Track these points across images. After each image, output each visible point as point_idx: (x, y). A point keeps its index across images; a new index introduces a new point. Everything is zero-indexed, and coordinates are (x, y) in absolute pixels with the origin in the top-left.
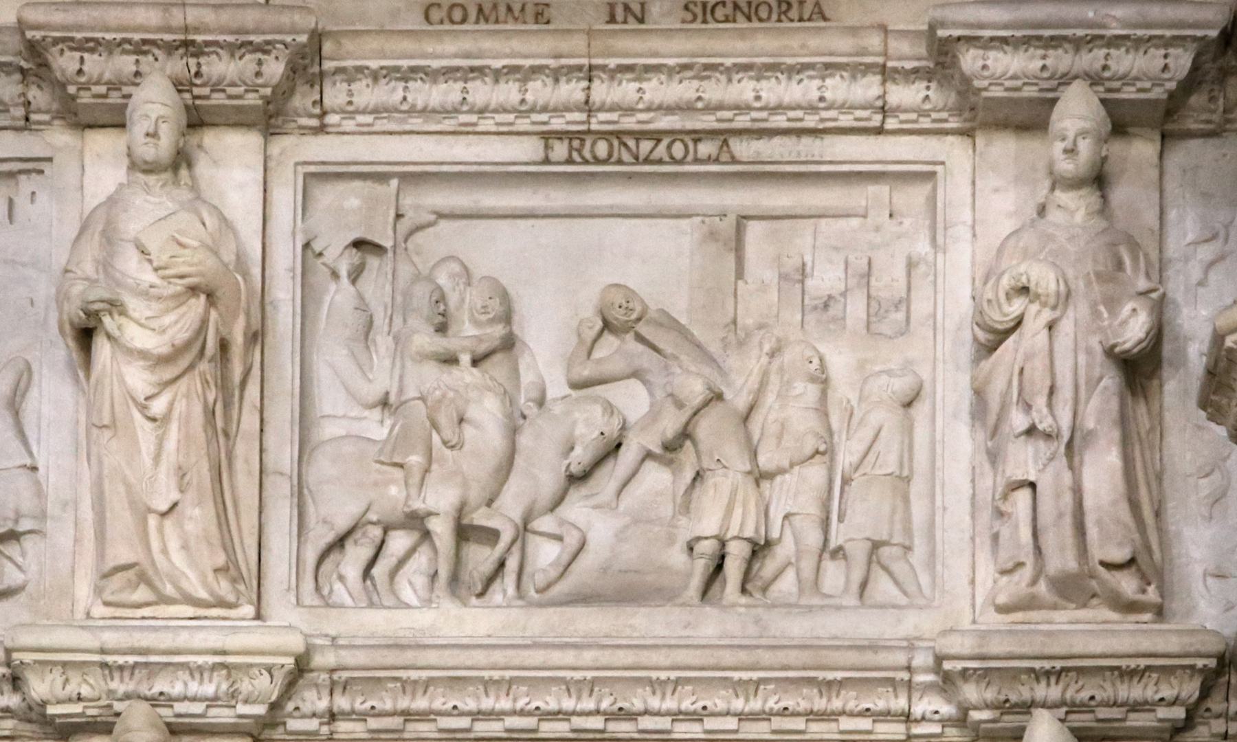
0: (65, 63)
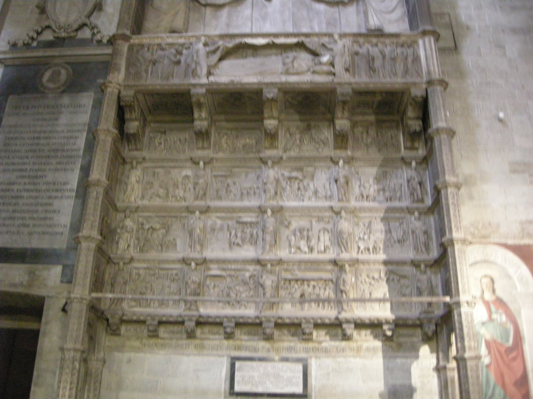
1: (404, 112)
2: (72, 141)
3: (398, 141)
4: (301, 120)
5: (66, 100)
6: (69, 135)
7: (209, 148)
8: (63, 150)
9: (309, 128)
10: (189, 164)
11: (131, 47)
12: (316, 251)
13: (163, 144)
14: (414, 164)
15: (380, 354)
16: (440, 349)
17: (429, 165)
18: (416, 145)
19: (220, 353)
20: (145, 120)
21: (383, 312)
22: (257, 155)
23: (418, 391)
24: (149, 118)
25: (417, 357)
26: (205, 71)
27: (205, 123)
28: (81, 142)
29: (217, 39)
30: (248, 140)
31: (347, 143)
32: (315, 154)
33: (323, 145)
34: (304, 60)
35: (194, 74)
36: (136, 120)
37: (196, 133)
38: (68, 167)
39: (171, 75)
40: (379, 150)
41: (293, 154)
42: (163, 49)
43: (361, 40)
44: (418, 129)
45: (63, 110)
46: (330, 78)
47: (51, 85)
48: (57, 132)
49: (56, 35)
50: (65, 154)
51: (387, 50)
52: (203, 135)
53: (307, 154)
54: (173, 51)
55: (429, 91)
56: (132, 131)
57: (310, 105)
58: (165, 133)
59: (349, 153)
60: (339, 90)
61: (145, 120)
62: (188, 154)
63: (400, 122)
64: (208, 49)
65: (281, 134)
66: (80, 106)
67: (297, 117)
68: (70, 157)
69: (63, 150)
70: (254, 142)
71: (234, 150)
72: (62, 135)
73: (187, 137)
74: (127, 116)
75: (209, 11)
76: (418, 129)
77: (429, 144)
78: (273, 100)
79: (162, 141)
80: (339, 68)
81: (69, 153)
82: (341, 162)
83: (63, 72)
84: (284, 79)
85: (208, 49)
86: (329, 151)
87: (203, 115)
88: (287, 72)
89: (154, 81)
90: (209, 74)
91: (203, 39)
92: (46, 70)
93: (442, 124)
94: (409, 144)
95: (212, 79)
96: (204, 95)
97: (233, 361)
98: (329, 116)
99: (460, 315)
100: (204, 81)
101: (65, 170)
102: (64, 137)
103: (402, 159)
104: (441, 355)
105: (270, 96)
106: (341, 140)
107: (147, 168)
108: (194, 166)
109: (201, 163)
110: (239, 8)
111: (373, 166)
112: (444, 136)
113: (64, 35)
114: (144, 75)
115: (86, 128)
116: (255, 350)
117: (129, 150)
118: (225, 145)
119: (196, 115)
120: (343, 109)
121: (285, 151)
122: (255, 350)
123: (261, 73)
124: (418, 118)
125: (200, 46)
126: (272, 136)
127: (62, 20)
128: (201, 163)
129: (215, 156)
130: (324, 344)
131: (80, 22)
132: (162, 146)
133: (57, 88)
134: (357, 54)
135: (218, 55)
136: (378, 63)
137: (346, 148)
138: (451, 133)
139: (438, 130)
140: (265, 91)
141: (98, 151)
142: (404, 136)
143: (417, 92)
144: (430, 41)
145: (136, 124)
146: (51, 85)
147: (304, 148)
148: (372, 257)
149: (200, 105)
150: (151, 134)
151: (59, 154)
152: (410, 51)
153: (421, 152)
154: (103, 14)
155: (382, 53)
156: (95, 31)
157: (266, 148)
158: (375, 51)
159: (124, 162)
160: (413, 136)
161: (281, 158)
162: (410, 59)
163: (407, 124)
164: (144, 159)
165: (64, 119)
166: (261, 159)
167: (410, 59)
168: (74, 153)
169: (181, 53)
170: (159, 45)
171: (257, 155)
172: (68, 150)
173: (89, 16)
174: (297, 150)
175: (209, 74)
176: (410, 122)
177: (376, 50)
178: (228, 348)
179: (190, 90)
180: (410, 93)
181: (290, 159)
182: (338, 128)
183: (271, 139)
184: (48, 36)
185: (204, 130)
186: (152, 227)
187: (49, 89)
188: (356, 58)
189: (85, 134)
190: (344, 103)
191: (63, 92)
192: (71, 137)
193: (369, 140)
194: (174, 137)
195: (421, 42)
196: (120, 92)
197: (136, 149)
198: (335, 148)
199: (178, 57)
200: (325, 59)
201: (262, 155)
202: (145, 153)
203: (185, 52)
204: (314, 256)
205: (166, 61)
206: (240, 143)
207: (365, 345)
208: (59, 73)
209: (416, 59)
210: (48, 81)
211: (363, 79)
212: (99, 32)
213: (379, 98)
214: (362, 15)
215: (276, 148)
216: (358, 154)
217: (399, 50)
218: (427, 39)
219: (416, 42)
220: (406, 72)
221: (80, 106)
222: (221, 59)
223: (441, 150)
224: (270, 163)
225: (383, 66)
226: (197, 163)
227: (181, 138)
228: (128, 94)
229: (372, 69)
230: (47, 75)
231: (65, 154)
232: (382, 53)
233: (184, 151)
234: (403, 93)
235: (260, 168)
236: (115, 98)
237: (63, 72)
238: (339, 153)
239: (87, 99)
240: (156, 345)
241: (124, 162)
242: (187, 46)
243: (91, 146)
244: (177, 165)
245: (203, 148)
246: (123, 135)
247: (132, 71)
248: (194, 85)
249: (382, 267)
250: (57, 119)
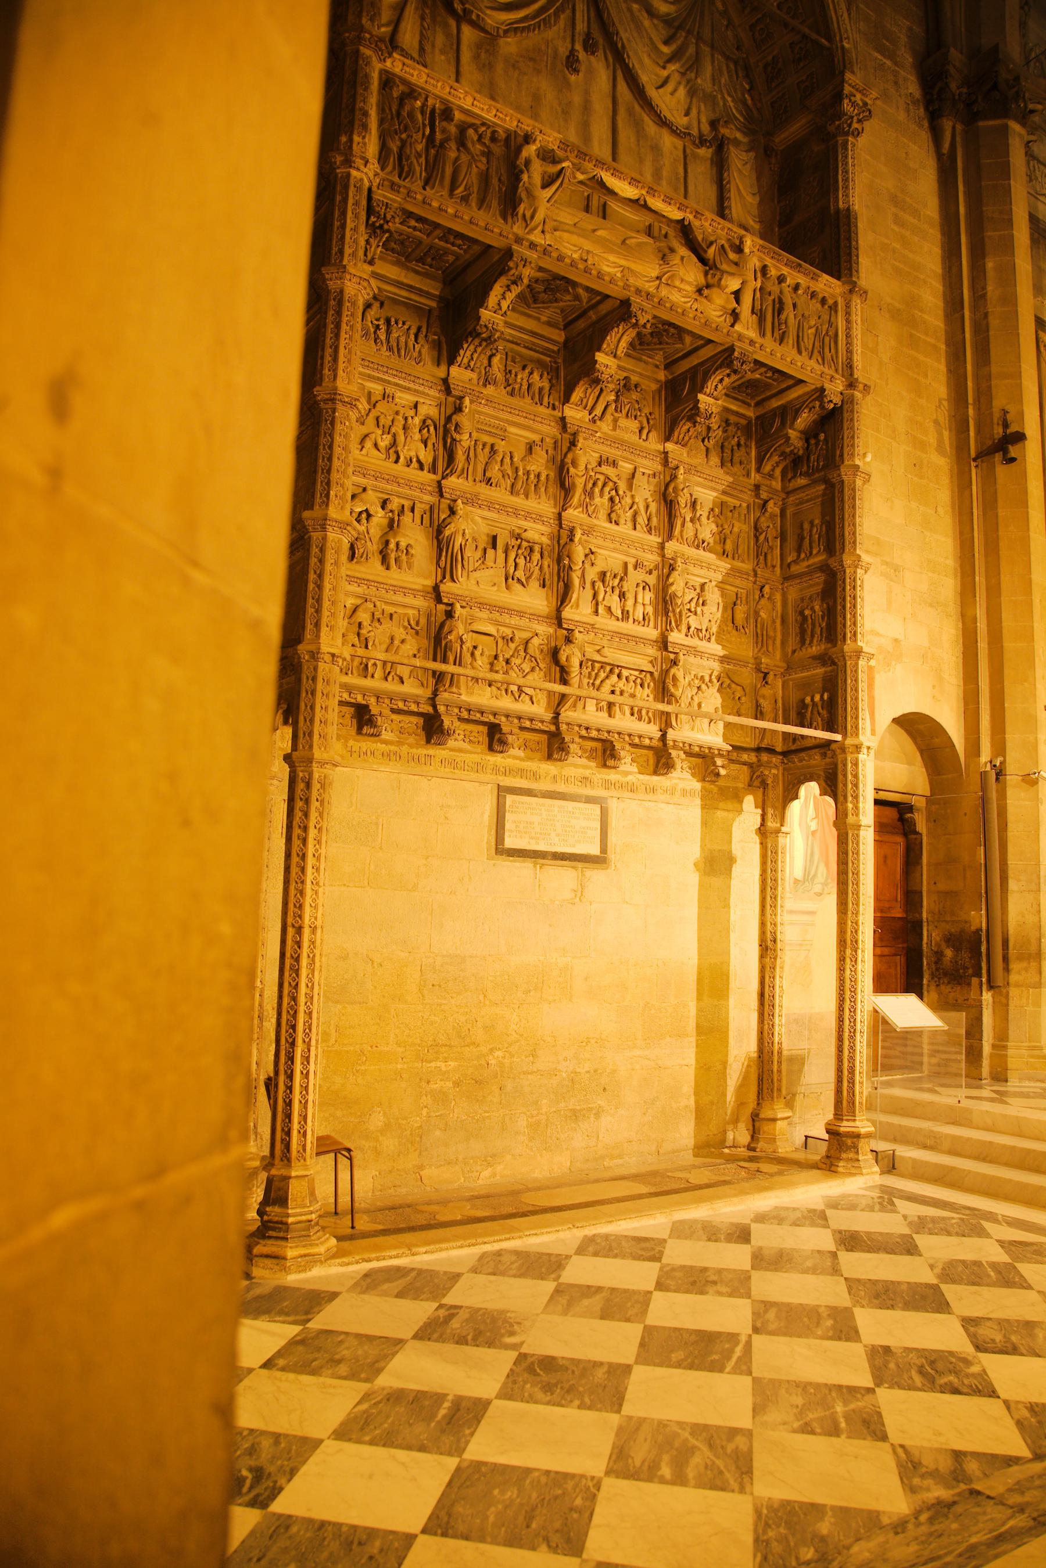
12: (631, 620)
15: (698, 802)
16: (768, 803)
19: (482, 777)
21: (711, 736)
23: (738, 861)
25: (740, 811)
97: (502, 791)
99: (856, 764)
104: (770, 811)
111: (714, 489)
116: (536, 776)
122: (536, 776)
130: (630, 778)
148: (703, 645)
178: (496, 770)
186: (367, 511)
204: (628, 627)
207: (681, 785)
240: (373, 753)
249: (716, 666)
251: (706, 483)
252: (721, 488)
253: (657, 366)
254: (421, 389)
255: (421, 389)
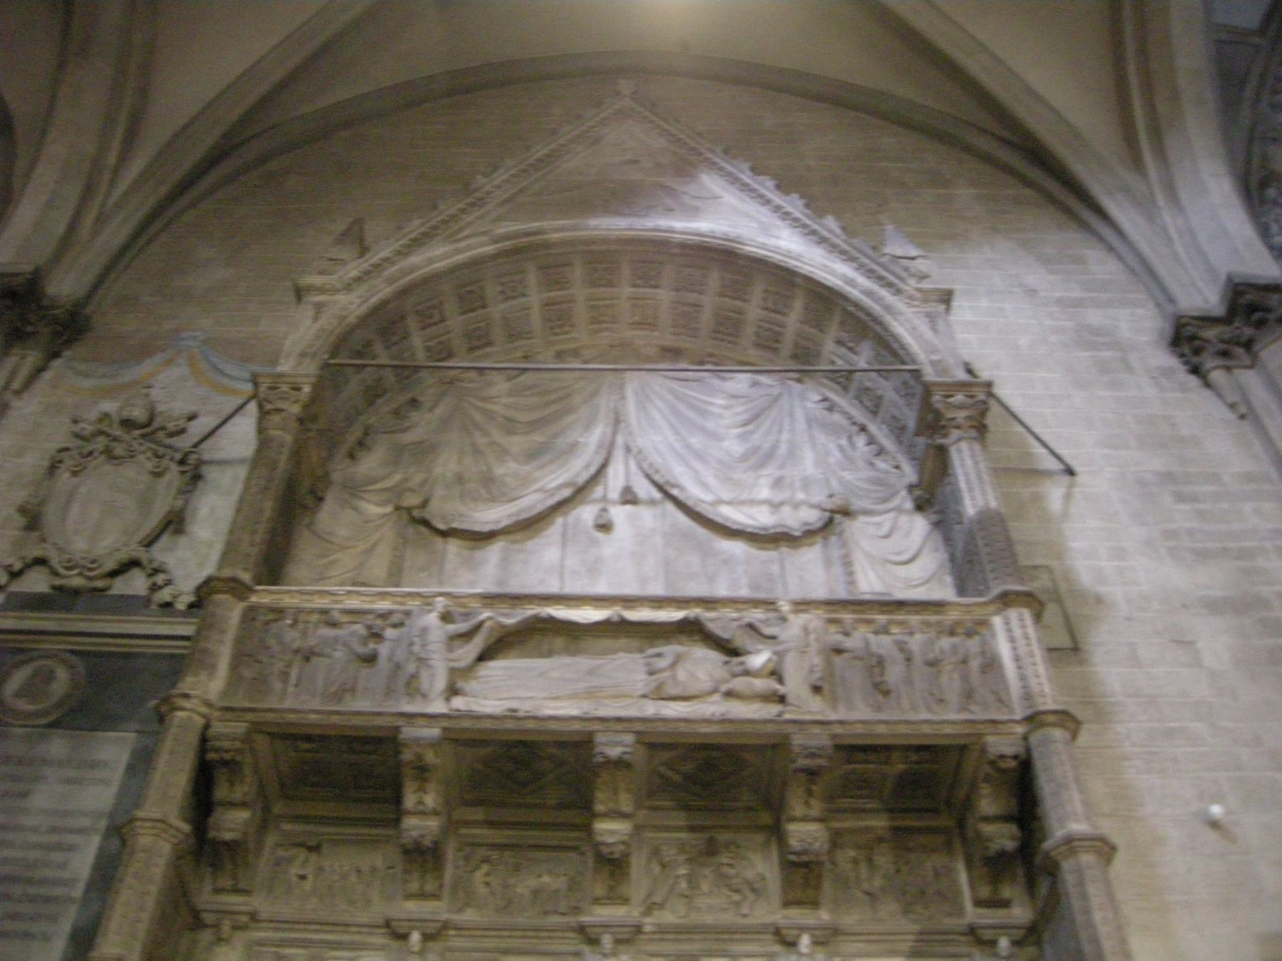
0: (784, 932)
1: (968, 804)
2: (57, 857)
3: (955, 882)
4: (692, 829)
5: (57, 746)
6: (54, 838)
7: (436, 896)
8: (30, 881)
9: (711, 850)
10: (379, 940)
11: (251, 614)
13: (311, 877)
14: (1004, 943)
17: (1047, 947)
18: (1006, 892)
20: (266, 809)
22: (572, 920)
24: (278, 808)
26: (441, 683)
27: (433, 824)
28: (83, 863)
29: (475, 604)
30: (546, 879)
31: (818, 888)
32: (728, 918)
33: (751, 896)
34: (701, 664)
35: (413, 688)
36: (244, 805)
37: (406, 852)
38: (35, 928)
39: (348, 689)
40: (906, 911)
41: (668, 917)
42: (334, 625)
43: (847, 617)
44: (1010, 845)
45: (48, 771)
46: (772, 710)
47: (24, 706)
48: (20, 828)
49: (58, 582)
50: (32, 890)
51: (916, 642)
52: (424, 857)
53: (709, 919)
54: (359, 629)
55: (1034, 739)
56: (228, 836)
57: (717, 783)
58: (315, 849)
59: (824, 916)
60: (798, 740)
61: (266, 809)
62: (379, 909)
63: (957, 830)
64: (452, 628)
65: (637, 863)
66: (93, 765)
67: (679, 818)
68: (48, 900)
69: (30, 881)
70: (560, 883)
71: (508, 906)
72: (35, 838)
73: (379, 863)
74: (221, 792)
75: (453, 547)
76: (1010, 845)
77: (1043, 888)
78: (620, 764)
79: (309, 870)
80: (795, 685)
81: (43, 891)
82: (805, 940)
83: (62, 674)
84: (651, 709)
85: (452, 628)
86: (768, 912)
87: (430, 800)
88: (659, 695)
89: (301, 700)
90: (453, 691)
91: (441, 602)
92: (16, 666)
93: (1078, 827)
94: (985, 892)
95: (458, 703)
96: (434, 744)
98: (766, 818)
100: (438, 707)
101: (27, 935)
102: (39, 846)
103: (972, 931)
105: (614, 752)
106: (803, 877)
107: (261, 943)
108: (394, 944)
109: (415, 937)
110: (530, 545)
112: (1087, 859)
113: (77, 582)
114: (278, 685)
115: (103, 823)
117: (217, 891)
118: (483, 891)
119: (409, 801)
120: (810, 793)
121: (648, 912)
123: (590, 694)
124: (1006, 818)
125: (432, 619)
126: (614, 866)
127: (79, 546)
128: (415, 937)
129: (455, 917)
131: (123, 555)
132: (308, 885)
133: (36, 714)
134: (838, 651)
135: (477, 644)
136: (894, 674)
137: (815, 904)
138: (1105, 849)
139: (1069, 840)
140: (600, 738)
141: (129, 880)
142: (969, 867)
143: (1003, 745)
144: (1020, 617)
145: (244, 815)
146: (24, 706)
147: (702, 902)
149: (422, 771)
150: (281, 853)
151: (17, 890)
152: (973, 644)
153: (1020, 913)
154: (183, 540)
155: (902, 647)
156: (160, 579)
157: (597, 901)
158: (883, 645)
159: (197, 923)
160: (996, 867)
161: (638, 929)
162: (975, 664)
163: (978, 835)
164: (254, 916)
165: (44, 797)
166: (582, 929)
167: (975, 664)
168: (58, 891)
169: (377, 636)
170: (324, 612)
171: (572, 920)
172: (43, 882)
173: (149, 543)
174: (681, 908)
175: (453, 691)
176: (988, 829)
177: (885, 639)
179: (397, 729)
180: (983, 750)
181: (663, 931)
182: (794, 843)
183: (612, 874)
184: (37, 582)
185: (427, 843)
187: (18, 714)
188: (837, 660)
189: (96, 840)
190: (812, 774)
191: (52, 725)
192: (58, 847)
193: (878, 882)
194: (342, 863)
195: (997, 621)
196: (207, 726)
197: (237, 891)
198: (787, 904)
199: (372, 645)
200: (758, 660)
201: (584, 919)
202: (258, 902)
203: (390, 633)
205: (339, 654)
206: (525, 885)
208: (49, 677)
209: (991, 665)
210: (18, 695)
211: (857, 713)
212: (168, 583)
213: (899, 766)
214: (838, 569)
215: (625, 901)
216: (849, 920)
217: (946, 642)
218: (1013, 614)
219: (984, 623)
220: (968, 695)
221: (93, 765)
222: (483, 657)
223: (1084, 897)
224: (607, 940)
225: (909, 681)
226: (403, 937)
227: (363, 869)
228: (228, 730)
229: (882, 690)
230: (18, 678)
231: (32, 890)
232: (902, 647)
233: (368, 902)
234: (963, 748)
235: (577, 954)
236: (194, 738)
237: (62, 674)
238: (797, 915)
239: (115, 749)
241: (197, 923)
242: (395, 619)
243: (106, 875)
244: (346, 938)
245: (422, 896)
246: (205, 850)
247: (248, 673)
248: (411, 716)
250: (24, 795)
251: (872, 948)
252: (905, 947)
253: (750, 809)
254: (357, 938)
255: (357, 938)
